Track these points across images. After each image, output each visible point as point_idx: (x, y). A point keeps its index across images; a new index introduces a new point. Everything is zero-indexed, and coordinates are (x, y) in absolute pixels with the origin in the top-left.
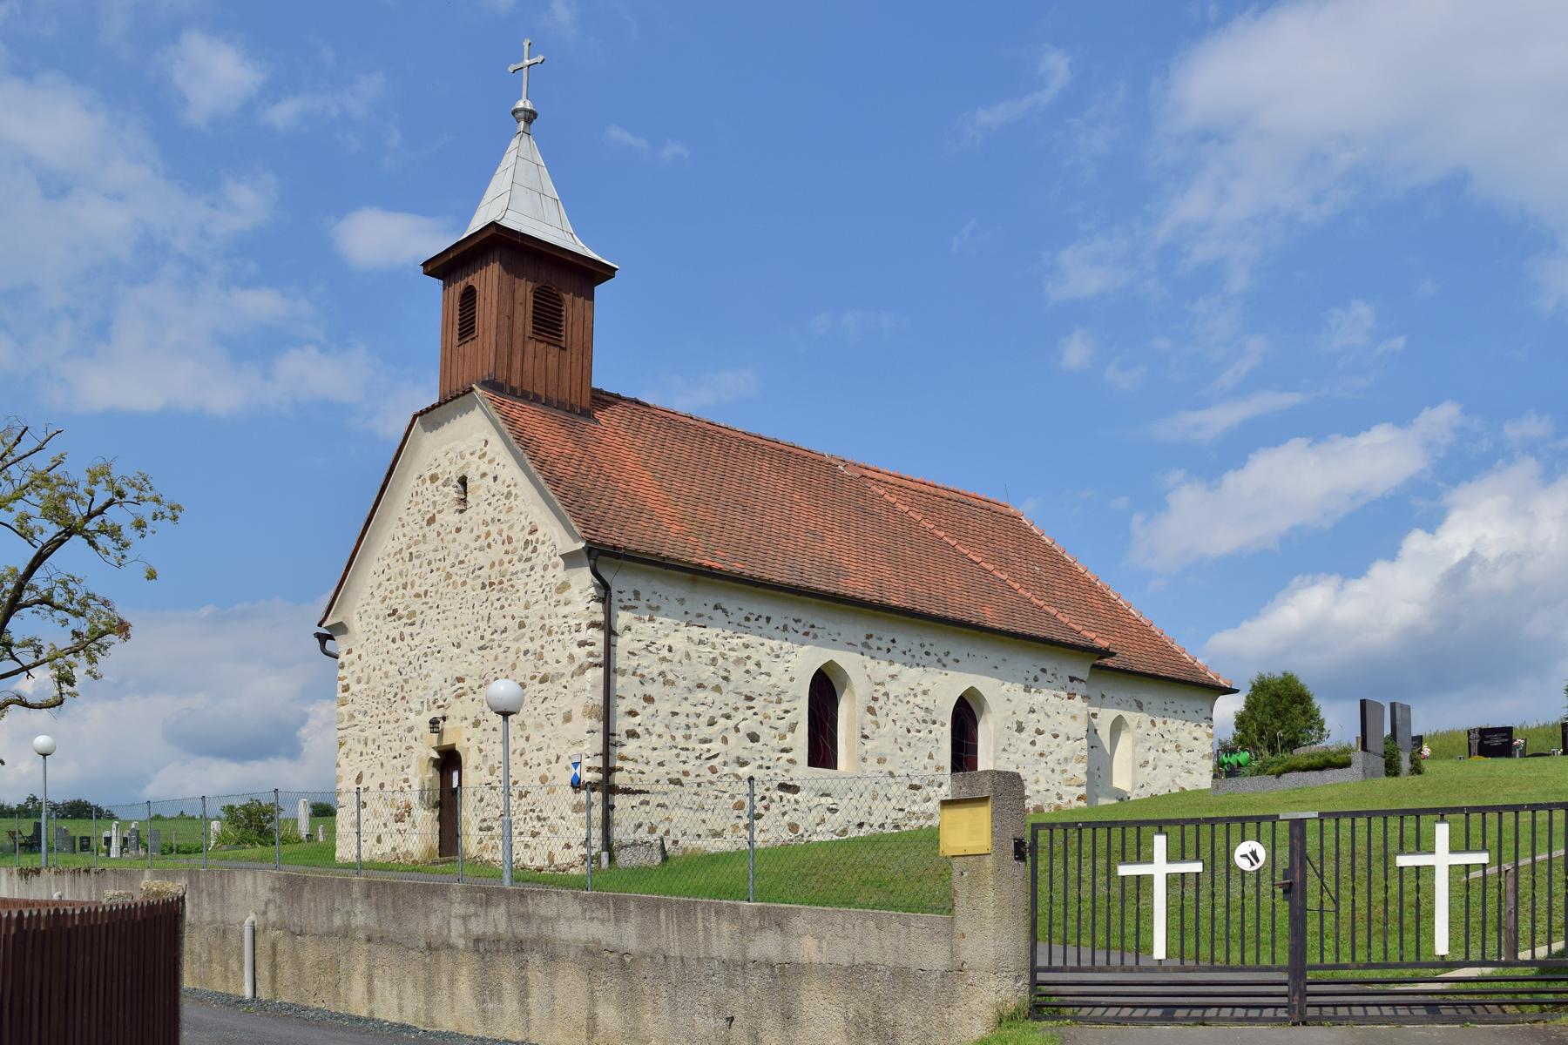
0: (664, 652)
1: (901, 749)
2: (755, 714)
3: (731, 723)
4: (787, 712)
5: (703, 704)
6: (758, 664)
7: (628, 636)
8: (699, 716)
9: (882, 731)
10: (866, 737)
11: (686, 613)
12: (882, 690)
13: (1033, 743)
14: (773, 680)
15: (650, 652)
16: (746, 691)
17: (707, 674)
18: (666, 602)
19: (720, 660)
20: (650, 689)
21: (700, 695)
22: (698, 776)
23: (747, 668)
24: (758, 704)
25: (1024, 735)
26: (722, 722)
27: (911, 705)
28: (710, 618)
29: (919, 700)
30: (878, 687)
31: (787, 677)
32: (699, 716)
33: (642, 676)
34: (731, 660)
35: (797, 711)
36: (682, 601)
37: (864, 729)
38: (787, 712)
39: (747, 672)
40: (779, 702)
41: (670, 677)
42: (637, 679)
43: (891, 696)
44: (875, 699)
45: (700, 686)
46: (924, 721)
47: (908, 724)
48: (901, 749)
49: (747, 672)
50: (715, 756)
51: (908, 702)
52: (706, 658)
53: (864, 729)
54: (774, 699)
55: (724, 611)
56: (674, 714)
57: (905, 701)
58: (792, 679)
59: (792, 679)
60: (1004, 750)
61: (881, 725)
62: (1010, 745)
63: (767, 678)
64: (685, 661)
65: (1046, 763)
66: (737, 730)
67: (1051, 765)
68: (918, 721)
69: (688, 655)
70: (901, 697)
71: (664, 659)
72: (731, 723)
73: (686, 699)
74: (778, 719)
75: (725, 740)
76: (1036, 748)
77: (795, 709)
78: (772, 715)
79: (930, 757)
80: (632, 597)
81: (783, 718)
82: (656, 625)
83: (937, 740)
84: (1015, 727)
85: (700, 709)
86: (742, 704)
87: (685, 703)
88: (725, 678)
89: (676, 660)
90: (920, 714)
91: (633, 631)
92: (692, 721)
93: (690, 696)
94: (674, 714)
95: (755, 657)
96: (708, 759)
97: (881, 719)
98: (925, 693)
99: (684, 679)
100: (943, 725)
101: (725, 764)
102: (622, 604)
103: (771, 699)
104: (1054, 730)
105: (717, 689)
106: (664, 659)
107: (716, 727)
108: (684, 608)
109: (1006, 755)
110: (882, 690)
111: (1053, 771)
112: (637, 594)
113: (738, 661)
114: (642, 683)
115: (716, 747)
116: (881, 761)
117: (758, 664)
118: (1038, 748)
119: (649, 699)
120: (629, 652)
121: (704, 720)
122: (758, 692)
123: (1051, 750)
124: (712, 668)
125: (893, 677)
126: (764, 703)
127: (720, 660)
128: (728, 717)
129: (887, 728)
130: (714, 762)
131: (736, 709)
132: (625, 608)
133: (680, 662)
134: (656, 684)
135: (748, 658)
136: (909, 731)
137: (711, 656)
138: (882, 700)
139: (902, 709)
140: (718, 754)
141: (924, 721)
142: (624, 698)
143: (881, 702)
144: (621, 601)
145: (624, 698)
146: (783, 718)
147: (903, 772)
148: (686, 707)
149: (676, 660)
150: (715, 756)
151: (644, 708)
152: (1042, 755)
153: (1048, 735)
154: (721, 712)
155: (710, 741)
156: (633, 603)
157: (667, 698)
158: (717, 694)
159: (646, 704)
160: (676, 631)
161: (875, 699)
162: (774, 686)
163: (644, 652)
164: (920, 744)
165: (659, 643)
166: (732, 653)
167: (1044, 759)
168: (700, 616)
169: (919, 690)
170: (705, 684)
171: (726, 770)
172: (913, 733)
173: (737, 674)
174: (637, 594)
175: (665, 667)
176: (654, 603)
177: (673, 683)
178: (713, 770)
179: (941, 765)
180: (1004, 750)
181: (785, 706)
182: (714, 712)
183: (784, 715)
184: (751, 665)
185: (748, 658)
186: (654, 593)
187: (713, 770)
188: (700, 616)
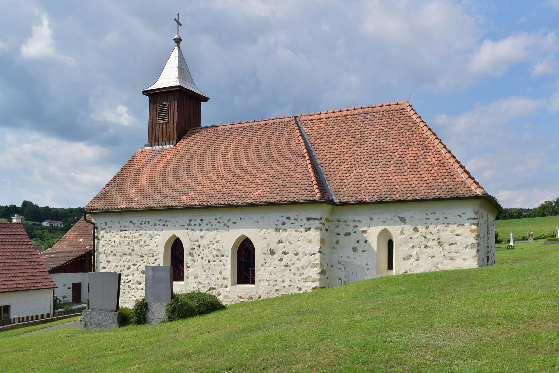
0: (113, 244)
1: (205, 271)
2: (144, 262)
3: (136, 267)
4: (156, 260)
5: (126, 261)
6: (145, 242)
7: (103, 239)
8: (125, 266)
9: (196, 263)
10: (189, 267)
11: (120, 227)
12: (197, 244)
13: (281, 260)
14: (150, 247)
15: (109, 244)
16: (140, 254)
17: (126, 249)
18: (114, 224)
19: (131, 243)
20: (110, 258)
21: (125, 258)
22: (124, 289)
23: (140, 244)
24: (145, 258)
25: (275, 256)
26: (133, 267)
27: (210, 249)
28: (128, 227)
29: (214, 246)
30: (195, 243)
31: (155, 245)
32: (125, 266)
33: (106, 253)
34: (134, 242)
35: (160, 259)
36: (119, 223)
37: (188, 263)
38: (156, 260)
39: (140, 246)
40: (153, 256)
41: (115, 252)
42: (105, 255)
43: (201, 246)
44: (193, 249)
45: (124, 254)
46: (217, 256)
47: (209, 258)
48: (205, 271)
49: (140, 246)
50: (130, 281)
51: (209, 248)
52: (126, 243)
53: (188, 263)
54: (151, 255)
55: (133, 223)
56: (117, 266)
57: (208, 247)
58: (157, 246)
59: (157, 246)
60: (262, 265)
61: (196, 261)
62: (266, 263)
63: (148, 247)
64: (119, 246)
65: (290, 270)
66: (137, 269)
67: (293, 271)
68: (214, 256)
69: (120, 243)
70: (206, 246)
71: (113, 246)
72: (136, 267)
73: (120, 260)
74: (153, 263)
75: (133, 275)
76: (282, 262)
77: (159, 258)
78: (150, 262)
79: (220, 273)
80: (104, 225)
81: (155, 263)
82: (111, 233)
83: (224, 265)
84: (269, 252)
85: (125, 263)
86: (139, 259)
87: (120, 262)
88: (133, 250)
89: (116, 246)
90: (215, 253)
91: (104, 237)
92: (123, 268)
93: (121, 259)
94: (117, 266)
95: (144, 239)
96: (127, 282)
97: (196, 257)
98: (217, 242)
99: (119, 252)
100: (227, 256)
101: (133, 284)
102: (101, 228)
103: (150, 255)
104: (295, 251)
105: (130, 254)
106: (113, 246)
107: (131, 270)
108: (120, 225)
109: (263, 268)
110: (197, 244)
111: (294, 274)
112: (106, 223)
113: (137, 242)
114: (107, 256)
115: (130, 278)
116: (196, 277)
117: (145, 242)
118: (284, 262)
119: (109, 262)
120: (103, 246)
121: (126, 267)
122: (144, 253)
123: (293, 262)
124: (128, 247)
125: (202, 237)
126: (147, 258)
127: (131, 243)
128: (135, 265)
129: (199, 262)
130: (130, 284)
131: (137, 261)
132: (102, 229)
133: (117, 246)
134: (111, 256)
135: (141, 240)
136: (209, 262)
137: (128, 242)
138: (196, 248)
139: (206, 252)
140: (131, 280)
141: (217, 256)
142: (102, 262)
143: (196, 250)
144: (101, 227)
145: (102, 262)
146: (155, 263)
147: (206, 282)
148: (121, 263)
149: (116, 246)
150: (130, 281)
151: (108, 265)
152: (286, 266)
153: (291, 254)
154: (132, 263)
155: (129, 275)
156: (104, 227)
157: (114, 260)
158: (130, 257)
159: (108, 264)
160: (117, 234)
161: (193, 249)
162: (151, 250)
163: (107, 245)
164: (215, 268)
165: (112, 240)
166: (136, 239)
167: (288, 268)
168: (125, 226)
169: (215, 241)
170: (126, 253)
171: (134, 286)
172: (212, 262)
173: (137, 247)
174: (106, 223)
175: (113, 249)
176: (110, 226)
177: (115, 255)
178: (129, 287)
179: (226, 277)
180: (262, 265)
181: (155, 257)
182: (130, 264)
183: (154, 262)
184: (142, 243)
185: (141, 240)
186: (111, 221)
187: (129, 287)
188: (125, 226)
